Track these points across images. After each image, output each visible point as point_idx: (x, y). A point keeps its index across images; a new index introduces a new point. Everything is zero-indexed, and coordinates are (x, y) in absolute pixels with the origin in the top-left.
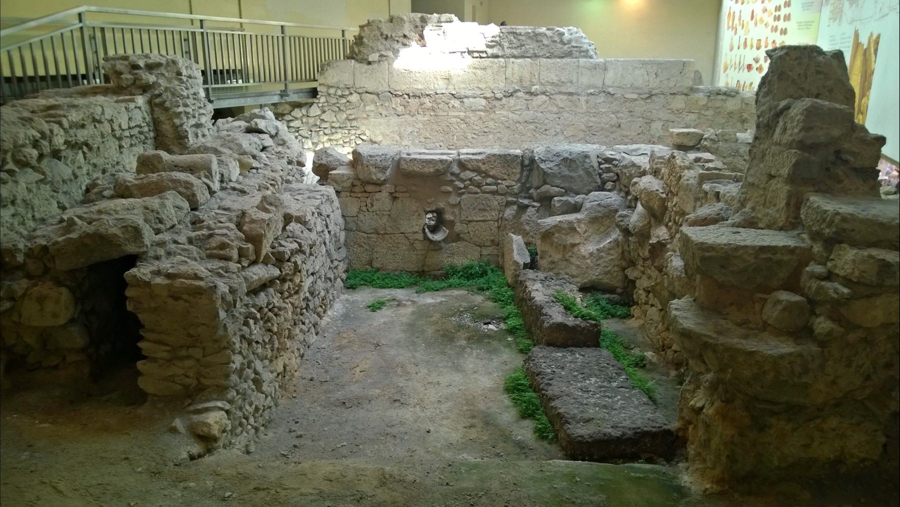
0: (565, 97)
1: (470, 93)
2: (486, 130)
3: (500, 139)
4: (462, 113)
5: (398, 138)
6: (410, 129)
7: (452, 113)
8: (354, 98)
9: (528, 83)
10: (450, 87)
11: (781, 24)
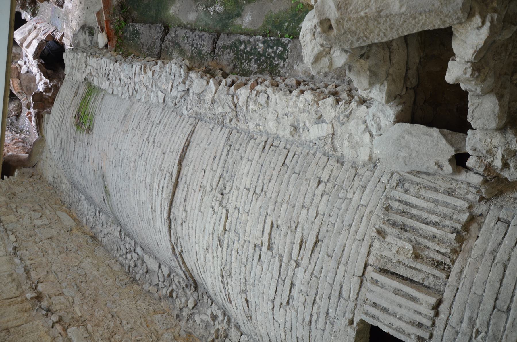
2: (110, 316)
9: (25, 304)
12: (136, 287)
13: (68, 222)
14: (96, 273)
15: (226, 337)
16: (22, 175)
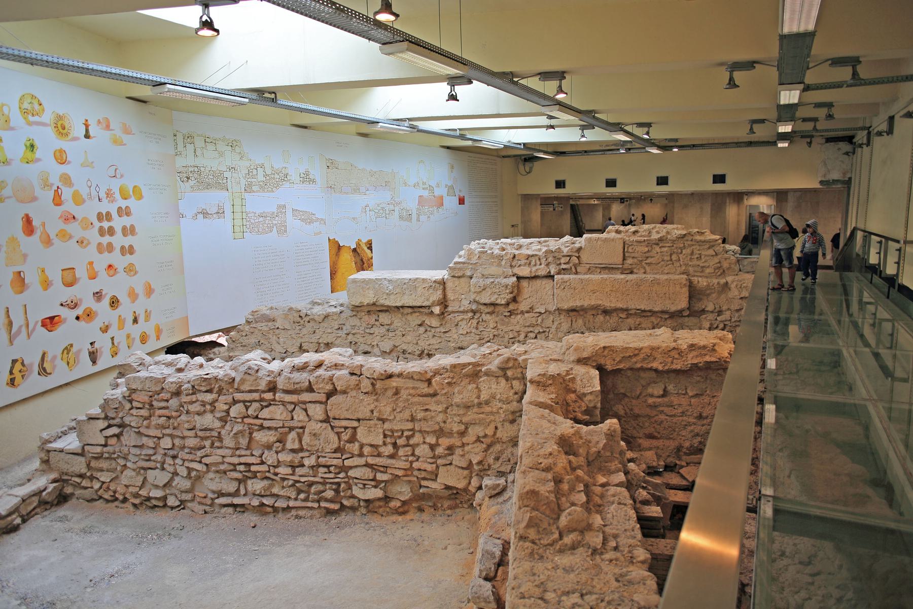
11: (118, 240)
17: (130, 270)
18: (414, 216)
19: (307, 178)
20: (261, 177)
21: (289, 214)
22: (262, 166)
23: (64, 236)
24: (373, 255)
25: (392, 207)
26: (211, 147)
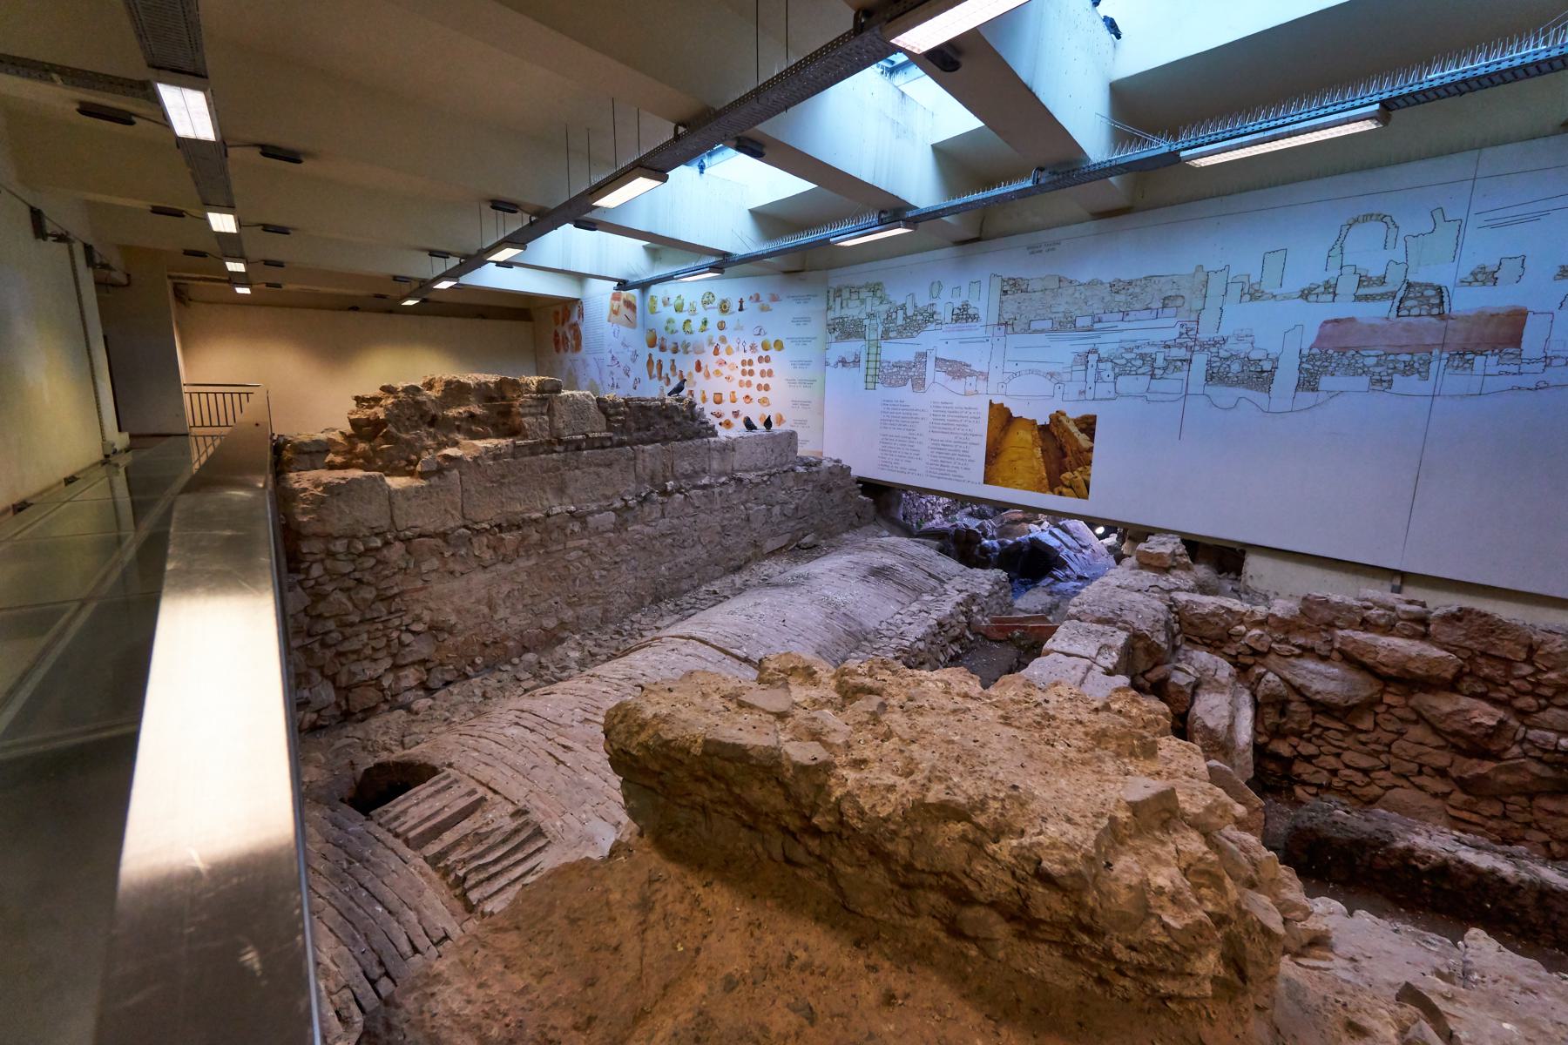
0: (700, 492)
1: (594, 507)
3: (635, 569)
4: (586, 541)
5: (486, 610)
6: (506, 589)
7: (570, 544)
8: (396, 552)
10: (566, 500)
11: (756, 379)
12: (649, 600)
13: (770, 545)
14: (682, 559)
15: (535, 676)
16: (865, 504)
17: (764, 401)
18: (1287, 375)
19: (964, 315)
20: (900, 321)
21: (931, 364)
22: (903, 307)
23: (717, 373)
24: (1096, 445)
25: (1182, 353)
26: (855, 296)
